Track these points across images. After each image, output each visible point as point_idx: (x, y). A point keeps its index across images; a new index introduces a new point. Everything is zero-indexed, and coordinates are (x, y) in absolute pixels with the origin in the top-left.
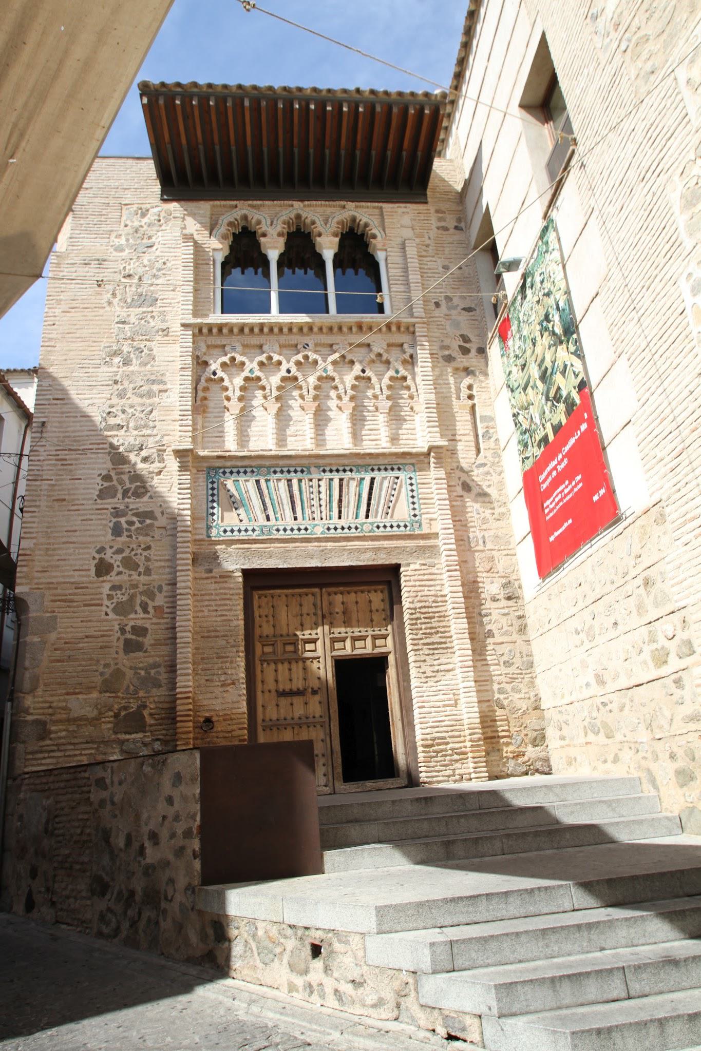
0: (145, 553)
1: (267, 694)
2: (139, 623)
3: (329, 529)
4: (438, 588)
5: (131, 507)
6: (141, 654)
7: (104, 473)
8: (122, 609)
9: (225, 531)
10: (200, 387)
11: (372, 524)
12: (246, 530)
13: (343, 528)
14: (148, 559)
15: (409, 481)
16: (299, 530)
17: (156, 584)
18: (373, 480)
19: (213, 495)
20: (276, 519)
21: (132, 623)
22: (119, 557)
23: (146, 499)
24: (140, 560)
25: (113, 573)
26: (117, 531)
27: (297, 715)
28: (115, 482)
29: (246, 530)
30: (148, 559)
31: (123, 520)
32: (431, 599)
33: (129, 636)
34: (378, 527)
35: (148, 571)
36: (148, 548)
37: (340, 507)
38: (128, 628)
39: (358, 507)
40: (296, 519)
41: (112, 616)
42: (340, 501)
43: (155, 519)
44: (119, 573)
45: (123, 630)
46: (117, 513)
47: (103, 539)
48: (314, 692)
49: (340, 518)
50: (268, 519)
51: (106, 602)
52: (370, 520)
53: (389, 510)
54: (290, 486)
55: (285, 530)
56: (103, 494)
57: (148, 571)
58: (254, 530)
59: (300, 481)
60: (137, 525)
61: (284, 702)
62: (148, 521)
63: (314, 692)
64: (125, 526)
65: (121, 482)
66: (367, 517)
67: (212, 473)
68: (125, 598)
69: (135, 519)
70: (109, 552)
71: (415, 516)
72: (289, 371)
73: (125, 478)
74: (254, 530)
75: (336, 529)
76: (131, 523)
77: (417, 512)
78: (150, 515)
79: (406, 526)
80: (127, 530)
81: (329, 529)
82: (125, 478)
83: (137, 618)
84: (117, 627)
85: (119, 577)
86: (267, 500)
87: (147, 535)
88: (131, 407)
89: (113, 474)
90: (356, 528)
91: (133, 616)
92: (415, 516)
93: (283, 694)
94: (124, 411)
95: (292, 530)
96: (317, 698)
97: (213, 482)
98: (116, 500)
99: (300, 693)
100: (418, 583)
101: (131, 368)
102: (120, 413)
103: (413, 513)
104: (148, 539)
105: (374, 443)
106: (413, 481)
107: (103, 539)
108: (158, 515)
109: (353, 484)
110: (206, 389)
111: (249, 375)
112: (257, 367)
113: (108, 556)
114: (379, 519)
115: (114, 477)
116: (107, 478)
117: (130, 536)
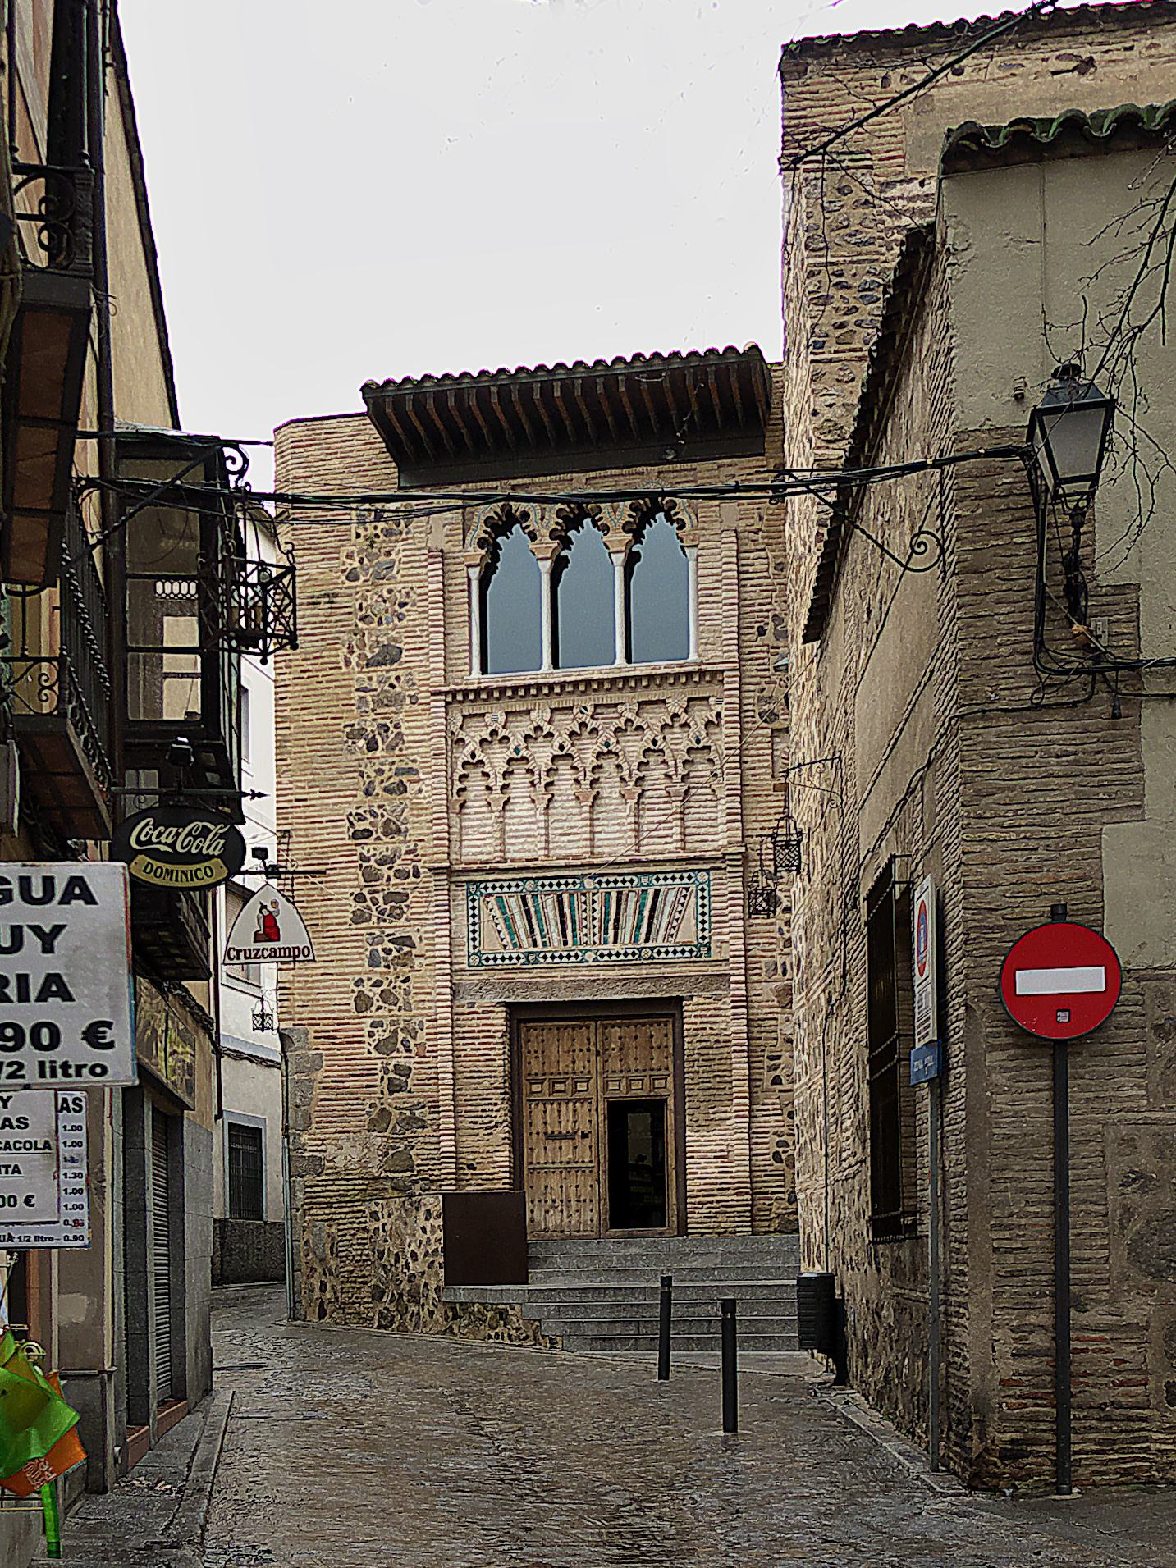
0: (404, 986)
1: (534, 1136)
2: (402, 1061)
3: (602, 956)
4: (723, 1026)
5: (387, 931)
6: (405, 1094)
7: (357, 891)
8: (385, 1047)
9: (487, 960)
10: (456, 776)
11: (652, 949)
12: (511, 958)
13: (618, 954)
14: (407, 992)
15: (700, 894)
16: (569, 957)
17: (417, 1020)
18: (657, 892)
19: (474, 916)
20: (544, 944)
21: (394, 1062)
22: (378, 990)
23: (402, 922)
24: (399, 993)
25: (373, 1008)
26: (373, 963)
27: (565, 1159)
28: (369, 903)
29: (511, 958)
30: (407, 992)
31: (379, 948)
32: (713, 1039)
33: (392, 1075)
34: (659, 953)
35: (408, 1006)
36: (407, 980)
37: (616, 928)
38: (391, 1068)
39: (639, 927)
40: (565, 943)
41: (375, 1054)
42: (617, 920)
43: (414, 946)
44: (379, 1008)
45: (386, 1070)
46: (374, 940)
47: (359, 969)
48: (585, 1136)
49: (615, 941)
50: (535, 944)
51: (367, 1039)
52: (650, 944)
53: (673, 927)
54: (561, 903)
55: (553, 957)
56: (359, 918)
57: (408, 1006)
58: (518, 958)
59: (571, 895)
60: (395, 953)
61: (550, 1144)
62: (406, 949)
63: (585, 1136)
64: (382, 954)
65: (375, 902)
66: (647, 940)
67: (473, 888)
68: (387, 1034)
69: (391, 946)
70: (367, 984)
71: (704, 938)
72: (561, 747)
73: (379, 896)
74: (518, 958)
75: (610, 955)
76: (388, 951)
77: (706, 934)
78: (407, 941)
79: (691, 951)
80: (386, 960)
81: (602, 956)
82: (379, 896)
83: (400, 1058)
84: (379, 1066)
85: (380, 1012)
86: (534, 921)
87: (404, 965)
88: (380, 807)
89: (365, 891)
90: (633, 954)
91: (395, 1054)
92: (704, 938)
93: (551, 1137)
94: (375, 815)
95: (561, 957)
96: (587, 1141)
97: (473, 900)
98: (370, 924)
99: (569, 1136)
100: (699, 1020)
101: (378, 753)
102: (368, 815)
103: (701, 934)
104: (407, 969)
105: (663, 840)
106: (706, 894)
107: (359, 969)
108: (416, 940)
109: (632, 897)
110: (463, 777)
111: (514, 755)
112: (523, 744)
113: (366, 988)
114: (660, 942)
115: (368, 897)
116: (360, 898)
117: (388, 967)
